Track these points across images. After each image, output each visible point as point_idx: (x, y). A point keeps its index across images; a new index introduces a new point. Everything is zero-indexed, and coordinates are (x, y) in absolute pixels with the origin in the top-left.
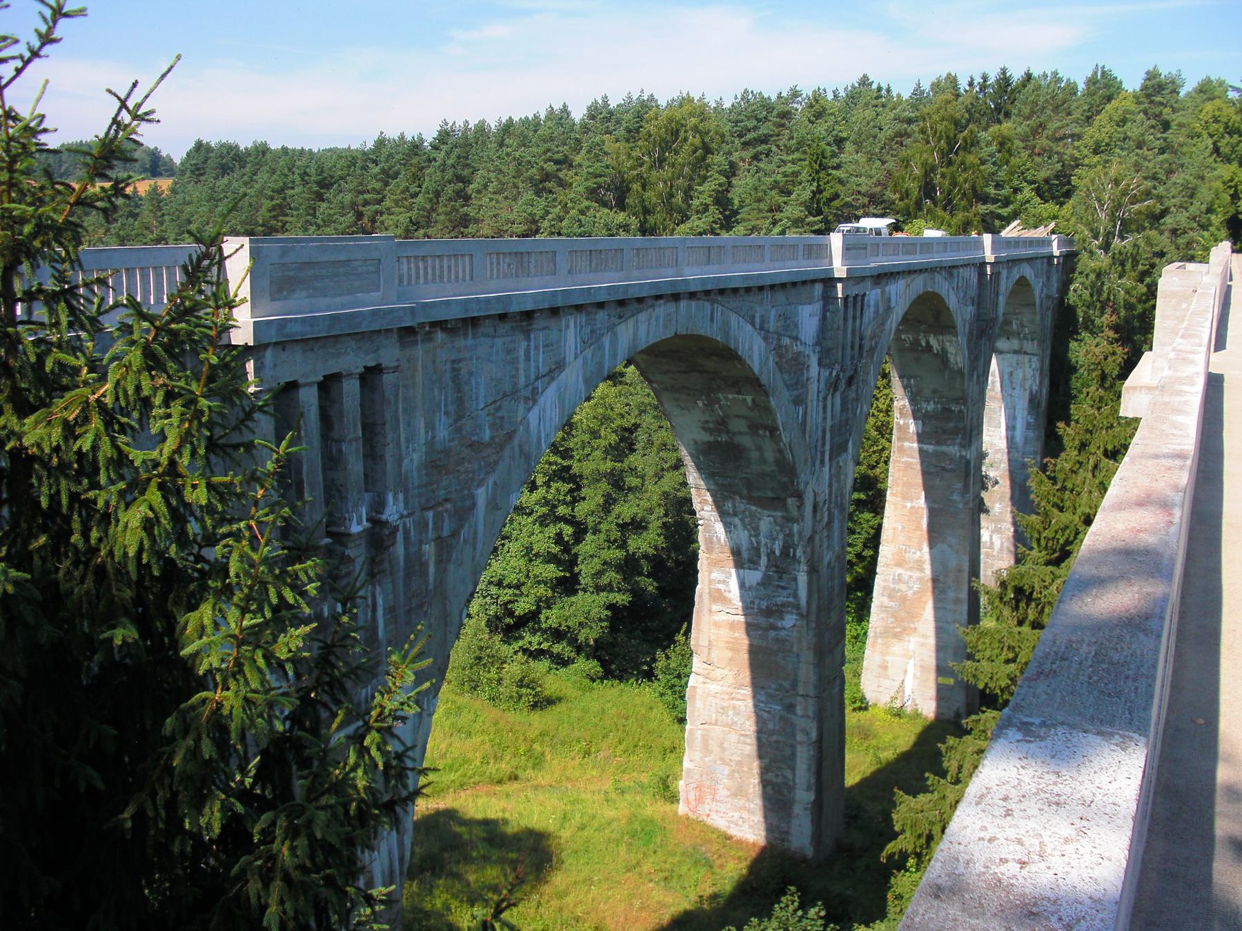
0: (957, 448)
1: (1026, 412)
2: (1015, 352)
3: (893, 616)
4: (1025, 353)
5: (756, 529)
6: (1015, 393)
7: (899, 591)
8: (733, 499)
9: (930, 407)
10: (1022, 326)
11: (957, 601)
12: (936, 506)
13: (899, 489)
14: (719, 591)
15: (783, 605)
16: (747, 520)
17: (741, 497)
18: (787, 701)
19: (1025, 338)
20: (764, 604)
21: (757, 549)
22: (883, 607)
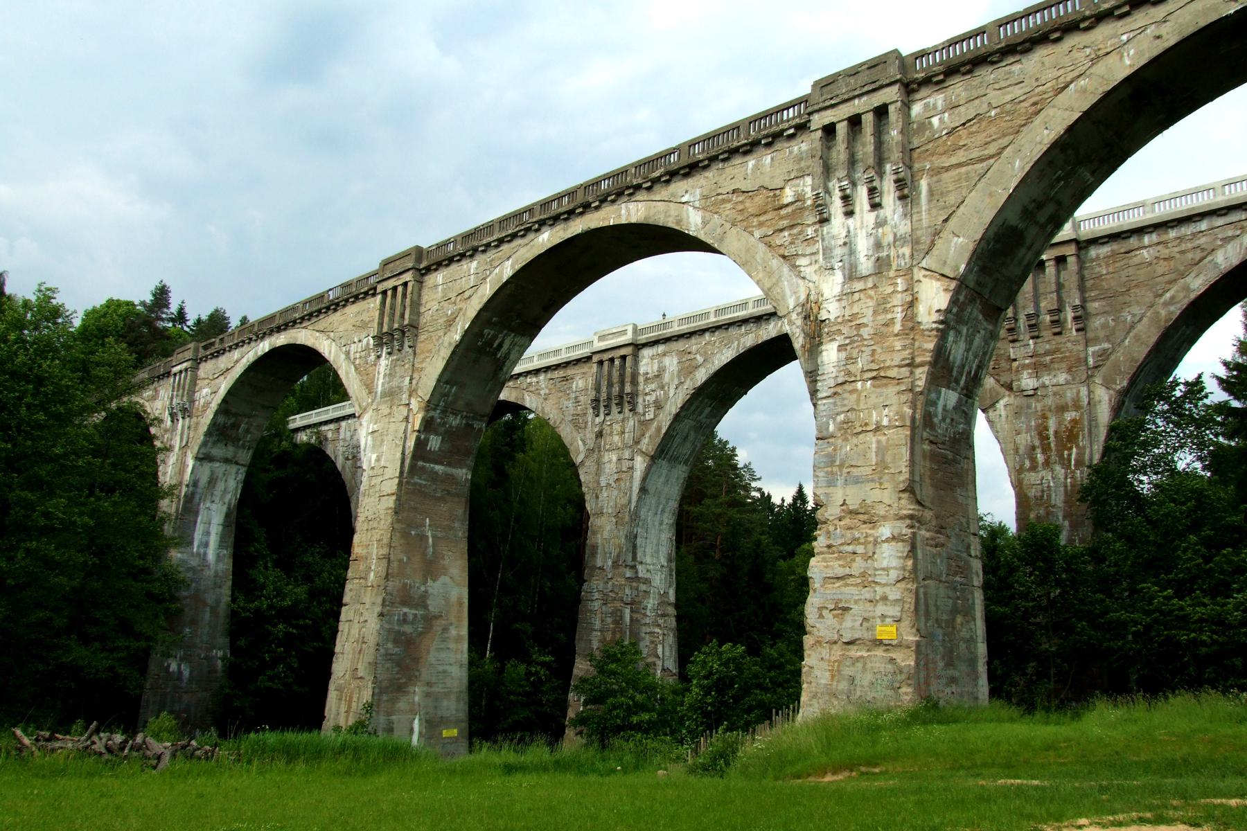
0: (464, 471)
1: (220, 528)
2: (227, 461)
3: (398, 665)
4: (237, 463)
6: (214, 507)
7: (404, 634)
9: (455, 421)
10: (247, 431)
11: (458, 639)
12: (440, 535)
13: (405, 514)
19: (243, 446)
22: (388, 656)
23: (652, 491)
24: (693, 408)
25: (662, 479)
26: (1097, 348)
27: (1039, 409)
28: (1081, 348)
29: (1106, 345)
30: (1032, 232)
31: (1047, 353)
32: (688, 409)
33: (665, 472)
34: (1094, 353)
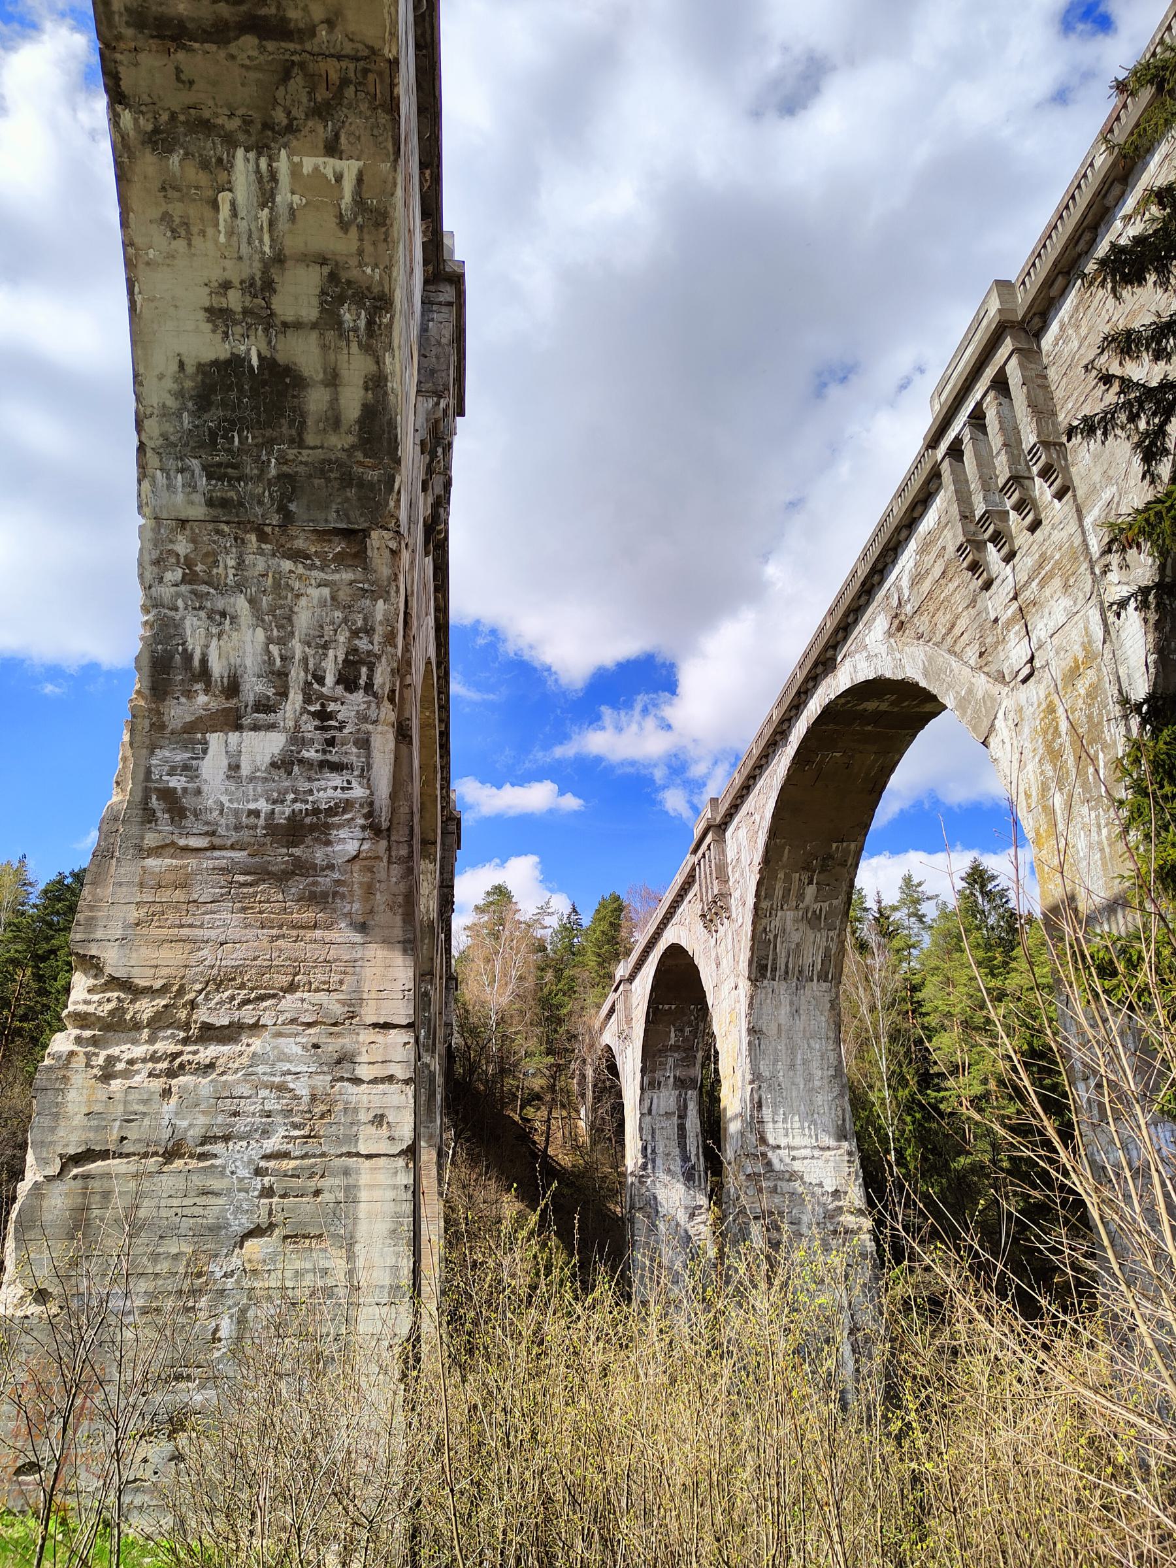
5: (287, 620)
8: (240, 541)
14: (168, 795)
15: (331, 812)
16: (265, 601)
17: (262, 537)
18: (332, 1046)
20: (283, 813)
21: (283, 675)
23: (772, 1030)
24: (778, 893)
25: (785, 1010)
26: (1096, 512)
27: (1042, 696)
28: (1073, 527)
29: (1106, 495)
30: (304, 353)
31: (1030, 579)
32: (769, 896)
33: (785, 999)
34: (1096, 525)
